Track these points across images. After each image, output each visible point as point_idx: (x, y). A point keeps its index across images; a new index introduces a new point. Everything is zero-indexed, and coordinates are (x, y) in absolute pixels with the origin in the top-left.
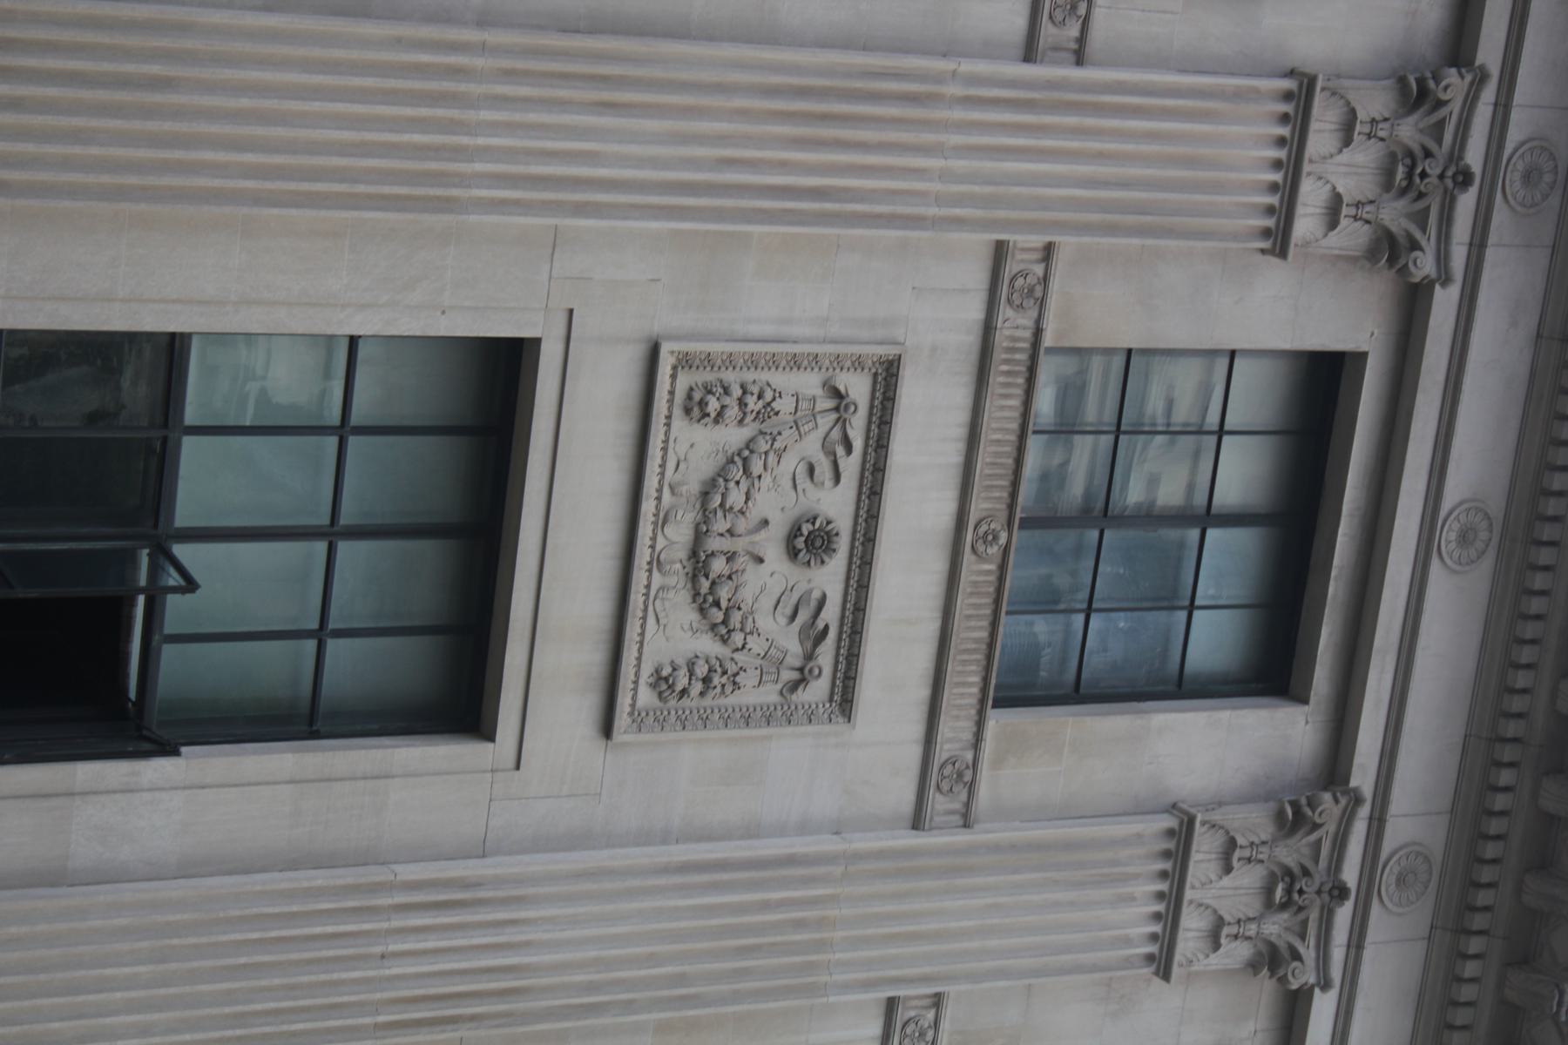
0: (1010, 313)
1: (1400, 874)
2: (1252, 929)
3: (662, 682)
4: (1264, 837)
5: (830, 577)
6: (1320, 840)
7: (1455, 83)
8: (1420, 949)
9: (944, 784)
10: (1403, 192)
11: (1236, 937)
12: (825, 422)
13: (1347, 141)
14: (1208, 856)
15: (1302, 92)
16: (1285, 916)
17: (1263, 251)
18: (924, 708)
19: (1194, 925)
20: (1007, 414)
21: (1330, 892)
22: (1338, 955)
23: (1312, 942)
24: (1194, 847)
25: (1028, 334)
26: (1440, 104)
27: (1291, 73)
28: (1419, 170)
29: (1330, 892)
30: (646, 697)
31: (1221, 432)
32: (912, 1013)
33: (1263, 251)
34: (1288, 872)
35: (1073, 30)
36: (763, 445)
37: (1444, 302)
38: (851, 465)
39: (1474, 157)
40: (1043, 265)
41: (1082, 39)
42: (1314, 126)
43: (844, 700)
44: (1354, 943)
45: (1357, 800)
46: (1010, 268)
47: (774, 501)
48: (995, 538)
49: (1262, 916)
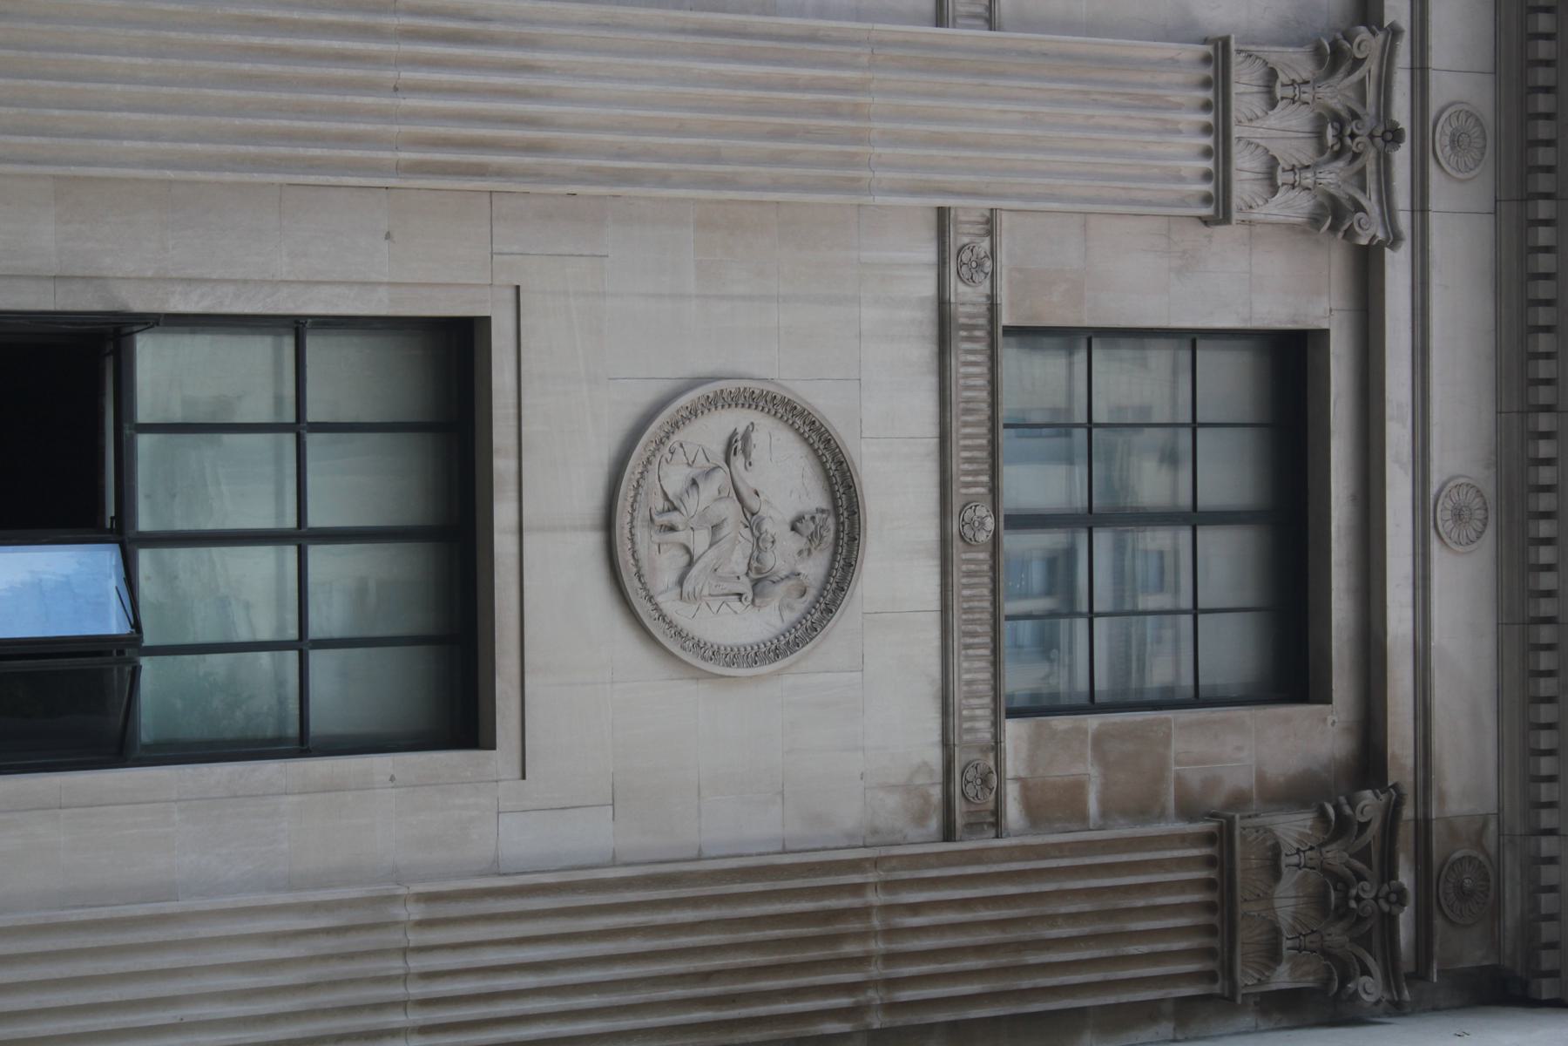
0: (962, 288)
1: (1453, 135)
2: (1308, 178)
4: (1306, 75)
6: (1362, 82)
7: (1367, 43)
8: (1486, 225)
10: (1337, 156)
11: (1293, 186)
13: (1273, 104)
14: (1250, 89)
15: (1219, 54)
16: (1340, 164)
17: (1206, 221)
18: (935, 456)
19: (1247, 166)
20: (977, 664)
21: (1383, 136)
22: (1402, 200)
23: (1374, 197)
24: (1233, 77)
25: (983, 309)
26: (1358, 63)
27: (1205, 41)
28: (1348, 131)
29: (1383, 136)
31: (1194, 425)
32: (966, 240)
33: (1206, 221)
34: (1336, 118)
35: (985, 288)
37: (1397, 269)
39: (1401, 112)
40: (987, 240)
41: (990, 8)
42: (1235, 89)
44: (1418, 206)
45: (1395, 32)
46: (956, 239)
48: (982, 524)
49: (1317, 165)
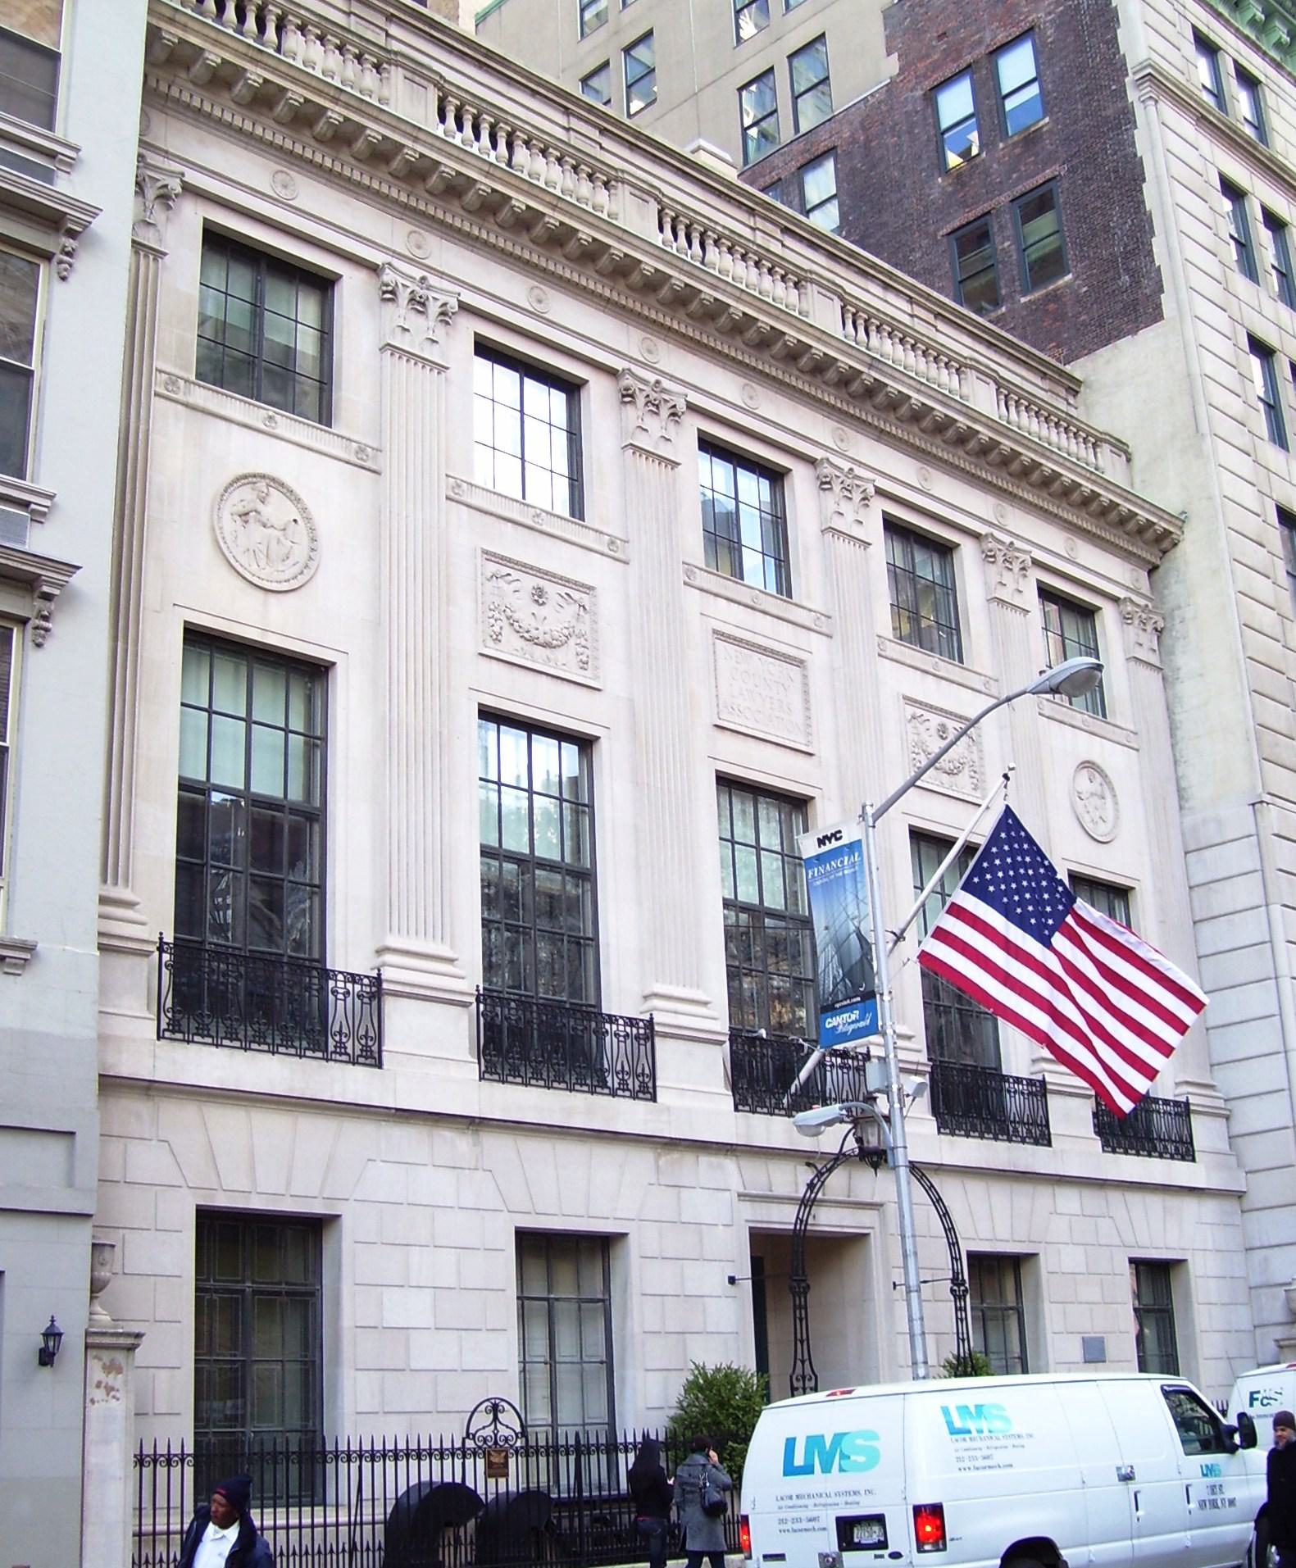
3: (584, 665)
5: (551, 589)
9: (615, 551)
12: (501, 582)
30: (587, 673)
36: (509, 612)
38: (515, 574)
43: (589, 589)
47: (524, 610)
